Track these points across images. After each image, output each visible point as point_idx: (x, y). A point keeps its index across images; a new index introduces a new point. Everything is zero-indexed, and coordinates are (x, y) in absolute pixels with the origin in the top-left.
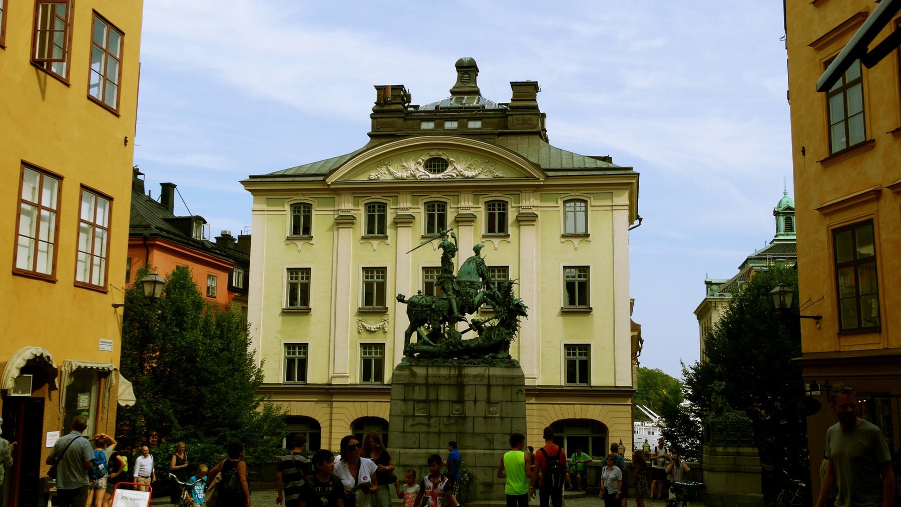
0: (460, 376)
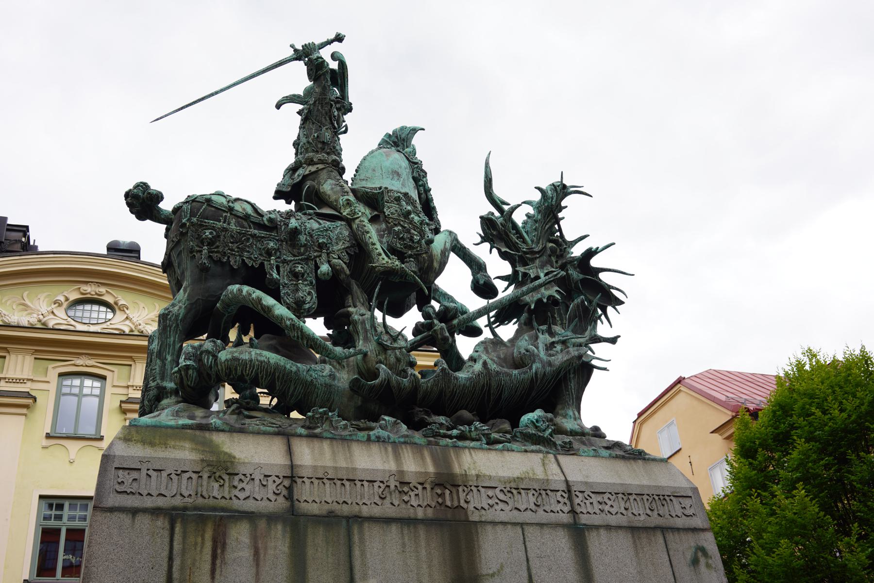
0: (446, 482)
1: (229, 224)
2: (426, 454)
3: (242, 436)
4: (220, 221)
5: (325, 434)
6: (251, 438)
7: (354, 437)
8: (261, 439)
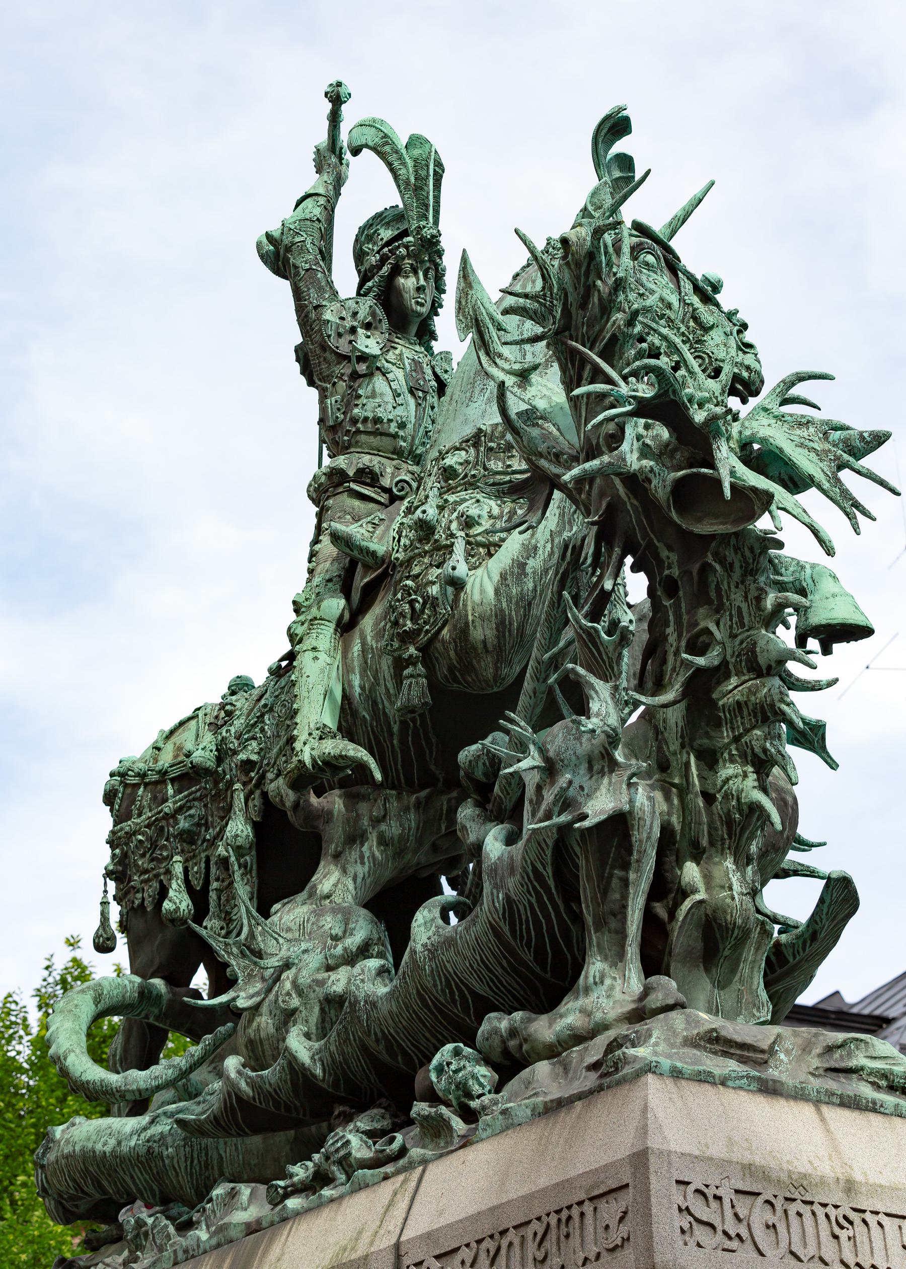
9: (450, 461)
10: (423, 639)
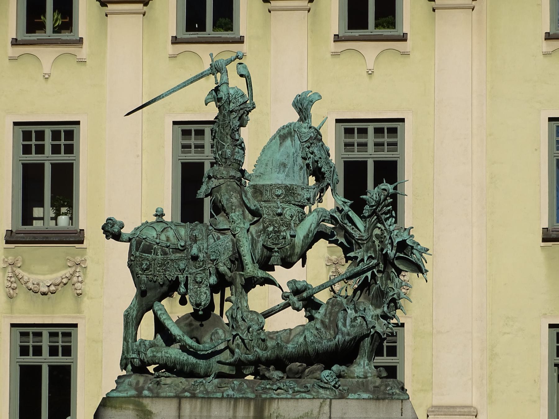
1: (157, 255)
2: (252, 404)
3: (157, 399)
4: (150, 253)
5: (200, 395)
6: (161, 400)
7: (215, 396)
8: (167, 401)
9: (279, 192)
10: (279, 246)
